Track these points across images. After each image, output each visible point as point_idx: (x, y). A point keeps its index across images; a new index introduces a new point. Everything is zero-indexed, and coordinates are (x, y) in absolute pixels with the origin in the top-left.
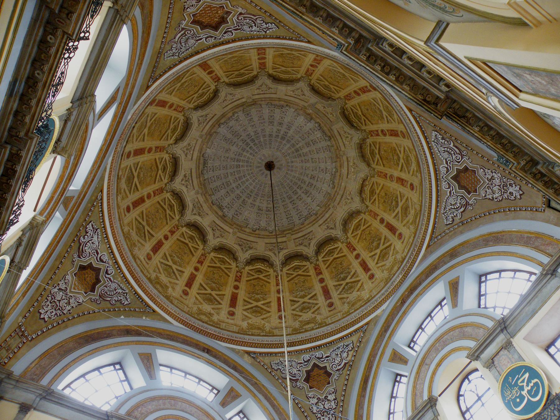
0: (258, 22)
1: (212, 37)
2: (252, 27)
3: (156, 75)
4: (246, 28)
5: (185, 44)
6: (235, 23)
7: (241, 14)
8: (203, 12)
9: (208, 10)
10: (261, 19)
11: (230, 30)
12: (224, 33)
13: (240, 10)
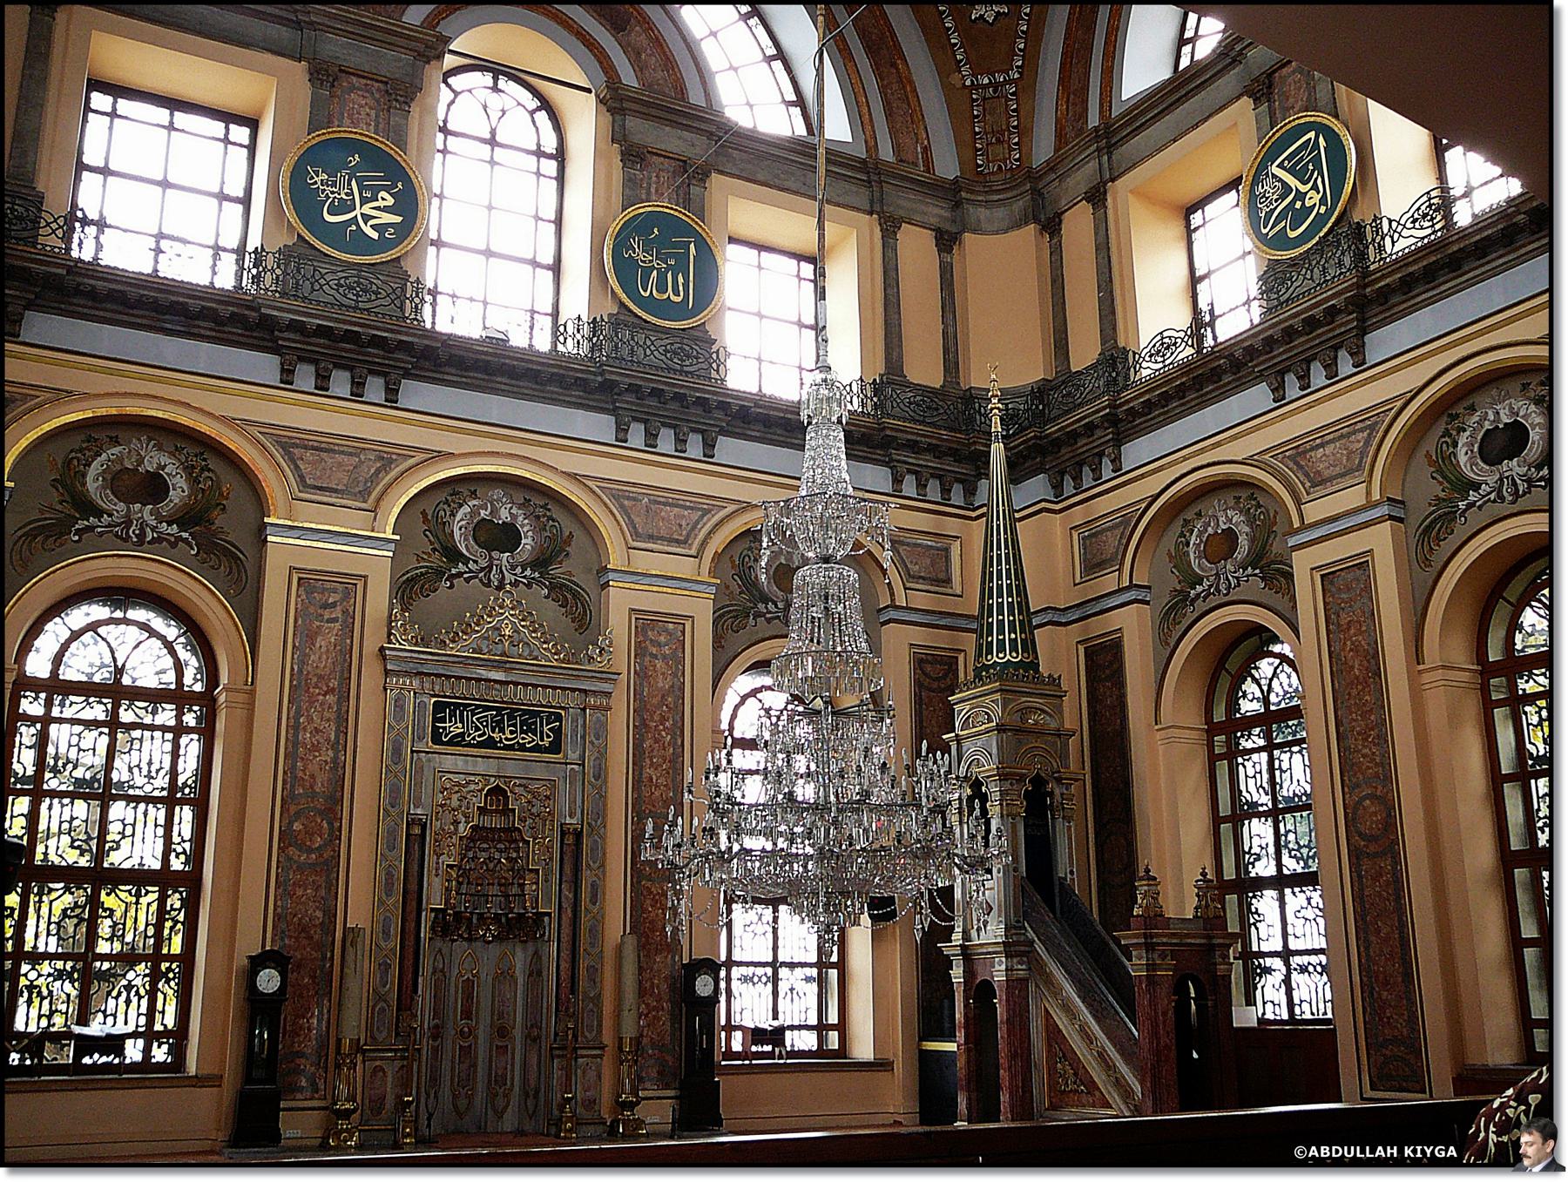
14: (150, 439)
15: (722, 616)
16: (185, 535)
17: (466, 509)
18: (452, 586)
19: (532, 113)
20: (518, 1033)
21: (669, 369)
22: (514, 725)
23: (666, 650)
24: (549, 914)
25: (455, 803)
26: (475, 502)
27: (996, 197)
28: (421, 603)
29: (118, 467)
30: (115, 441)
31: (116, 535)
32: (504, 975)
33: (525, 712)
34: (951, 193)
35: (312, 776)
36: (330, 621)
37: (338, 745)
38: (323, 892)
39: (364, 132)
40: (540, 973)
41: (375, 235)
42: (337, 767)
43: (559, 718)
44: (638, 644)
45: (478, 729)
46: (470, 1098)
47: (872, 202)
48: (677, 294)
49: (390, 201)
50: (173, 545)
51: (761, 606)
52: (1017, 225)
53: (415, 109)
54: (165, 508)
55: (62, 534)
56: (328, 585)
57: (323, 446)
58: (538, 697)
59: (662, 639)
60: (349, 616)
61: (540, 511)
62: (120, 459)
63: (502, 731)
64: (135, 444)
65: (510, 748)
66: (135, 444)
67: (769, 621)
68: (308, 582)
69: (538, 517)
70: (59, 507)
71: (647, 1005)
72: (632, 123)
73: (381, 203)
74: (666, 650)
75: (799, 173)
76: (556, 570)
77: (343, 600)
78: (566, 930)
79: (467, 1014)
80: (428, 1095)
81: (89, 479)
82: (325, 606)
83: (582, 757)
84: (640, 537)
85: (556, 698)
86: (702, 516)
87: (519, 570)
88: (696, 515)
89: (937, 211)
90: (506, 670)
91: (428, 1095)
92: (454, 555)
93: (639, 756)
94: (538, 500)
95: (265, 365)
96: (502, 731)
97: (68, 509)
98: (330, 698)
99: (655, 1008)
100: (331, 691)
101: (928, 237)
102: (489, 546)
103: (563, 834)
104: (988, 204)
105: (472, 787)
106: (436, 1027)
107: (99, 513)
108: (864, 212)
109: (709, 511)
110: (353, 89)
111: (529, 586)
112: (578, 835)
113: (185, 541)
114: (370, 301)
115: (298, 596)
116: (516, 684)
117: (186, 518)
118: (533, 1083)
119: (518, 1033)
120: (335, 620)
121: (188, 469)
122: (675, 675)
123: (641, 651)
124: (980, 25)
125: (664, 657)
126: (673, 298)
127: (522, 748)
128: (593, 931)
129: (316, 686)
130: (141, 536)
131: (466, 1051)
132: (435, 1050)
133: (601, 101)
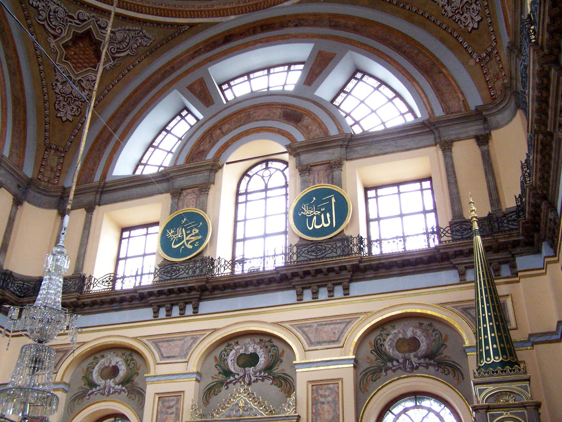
0: (44, 15)
1: (99, 25)
2: (55, 12)
3: (173, 30)
4: (61, 14)
5: (126, 38)
6: (67, 27)
7: (55, 37)
8: (85, 64)
9: (80, 63)
10: (40, 17)
11: (77, 22)
12: (85, 20)
13: (53, 42)
14: (114, 353)
15: (366, 374)
16: (124, 388)
17: (234, 351)
18: (227, 388)
19: (282, 171)
21: (310, 260)
23: (330, 399)
26: (238, 347)
27: (501, 106)
28: (214, 400)
29: (103, 366)
30: (103, 357)
31: (101, 394)
34: (480, 115)
39: (192, 209)
41: (191, 247)
44: (314, 399)
47: (435, 139)
48: (326, 222)
49: (197, 231)
50: (120, 393)
51: (389, 364)
52: (514, 115)
53: (211, 192)
54: (118, 379)
55: (84, 397)
56: (171, 398)
57: (169, 339)
59: (327, 393)
60: (178, 409)
61: (267, 344)
62: (104, 363)
64: (109, 356)
66: (109, 356)
67: (394, 371)
68: (162, 397)
69: (267, 347)
70: (84, 387)
72: (303, 157)
73: (194, 233)
74: (330, 399)
75: (392, 143)
76: (277, 370)
77: (176, 403)
81: (94, 373)
82: (169, 407)
84: (313, 343)
86: (347, 325)
87: (258, 374)
88: (342, 326)
89: (474, 128)
92: (227, 373)
94: (266, 339)
95: (148, 312)
97: (87, 387)
101: (472, 143)
102: (243, 366)
104: (499, 112)
107: (95, 385)
108: (432, 145)
109: (350, 322)
110: (188, 194)
111: (263, 380)
113: (124, 391)
114: (176, 274)
115: (158, 405)
117: (127, 381)
120: (172, 413)
121: (126, 361)
122: (334, 410)
123: (315, 402)
124: (474, 32)
125: (328, 402)
126: (326, 225)
130: (109, 392)
133: (290, 154)
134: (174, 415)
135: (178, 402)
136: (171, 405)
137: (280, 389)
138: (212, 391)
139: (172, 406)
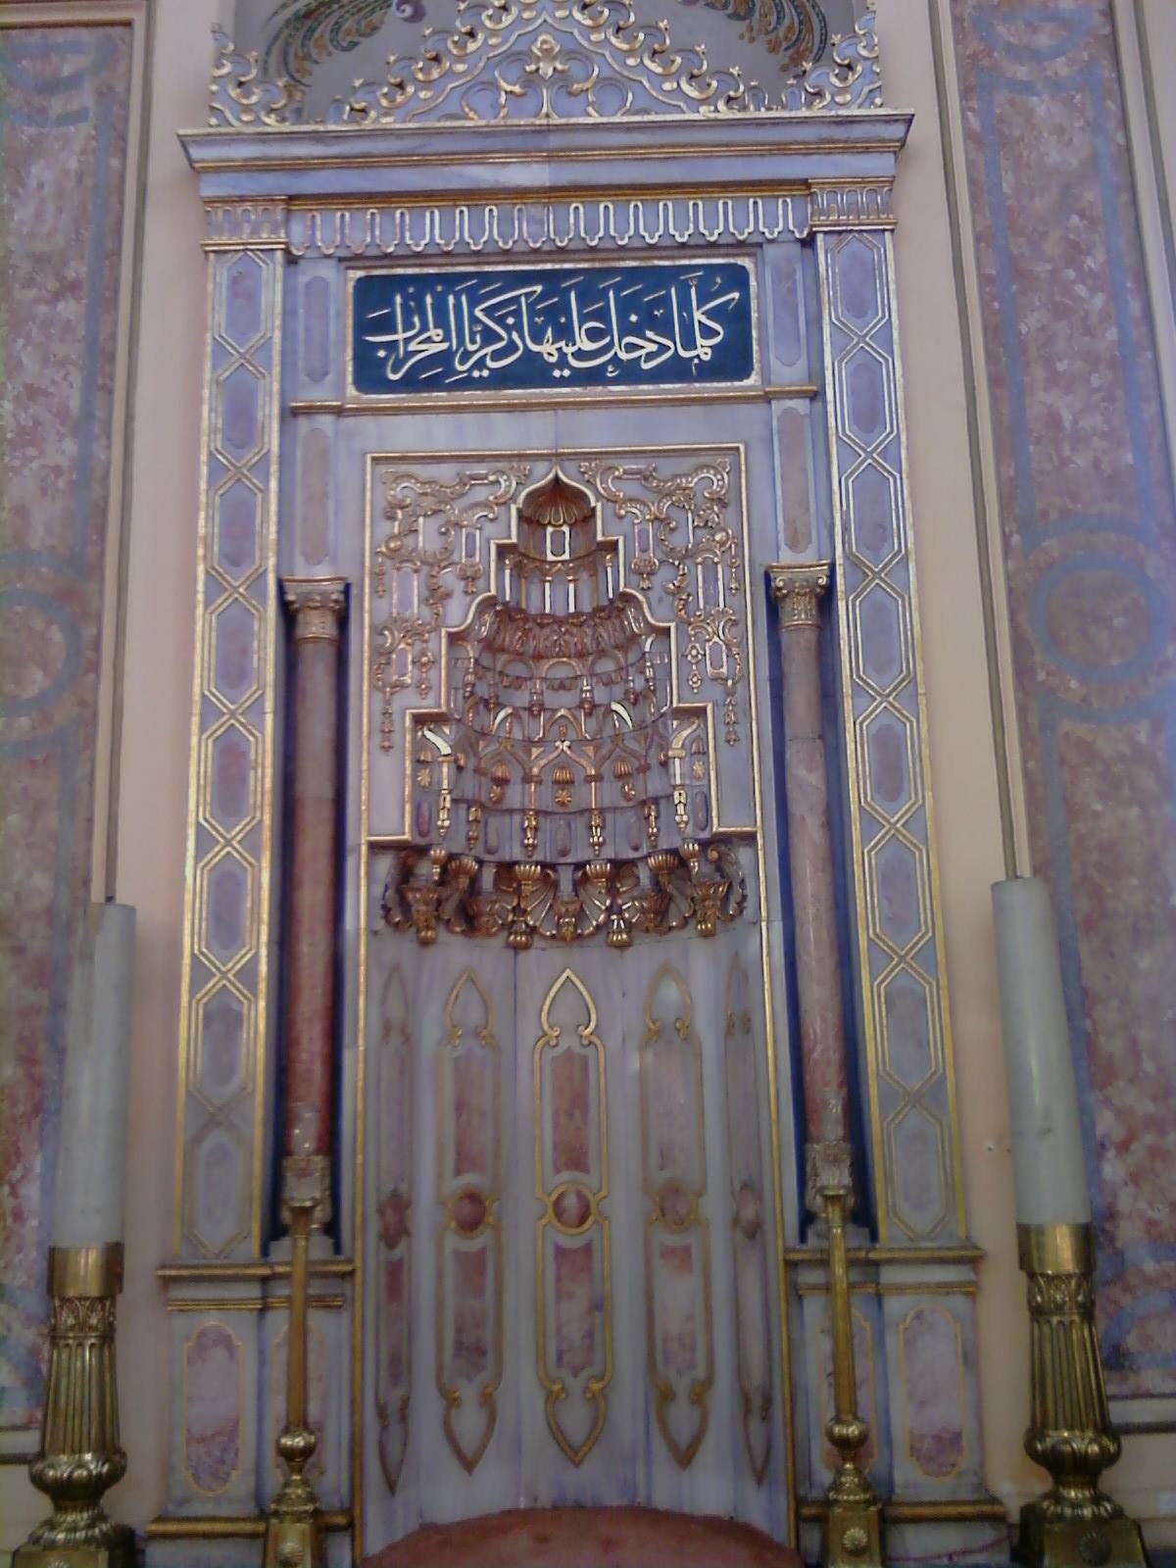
20: (715, 1207)
22: (602, 315)
23: (1061, 67)
24: (750, 838)
25: (426, 537)
32: (667, 1034)
33: (632, 275)
35: (21, 512)
36: (65, 119)
37: (87, 425)
38: (52, 820)
40: (747, 1029)
42: (87, 477)
43: (737, 278)
44: (970, 64)
45: (489, 337)
46: (598, 1404)
56: (59, 36)
58: (664, 223)
59: (1043, 40)
63: (565, 333)
65: (595, 377)
71: (1122, 1114)
74: (1061, 67)
78: (811, 884)
79: (574, 1157)
80: (451, 1402)
82: (52, 86)
83: (816, 373)
85: (721, 219)
90: (551, 157)
91: (451, 1402)
93: (1005, 357)
96: (565, 333)
98: (70, 309)
99: (1152, 1123)
100: (73, 288)
103: (774, 605)
105: (481, 494)
106: (473, 1197)
112: (825, 600)
116: (591, 192)
118: (756, 1376)
119: (715, 1207)
120: (80, 116)
125: (1056, 86)
127: (630, 373)
128: (897, 877)
129: (30, 282)
131: (576, 1262)
132: (474, 1268)
134: (86, 128)
135: (109, 58)
136: (67, 70)
137: (741, 26)
138: (324, 29)
139: (75, 81)
